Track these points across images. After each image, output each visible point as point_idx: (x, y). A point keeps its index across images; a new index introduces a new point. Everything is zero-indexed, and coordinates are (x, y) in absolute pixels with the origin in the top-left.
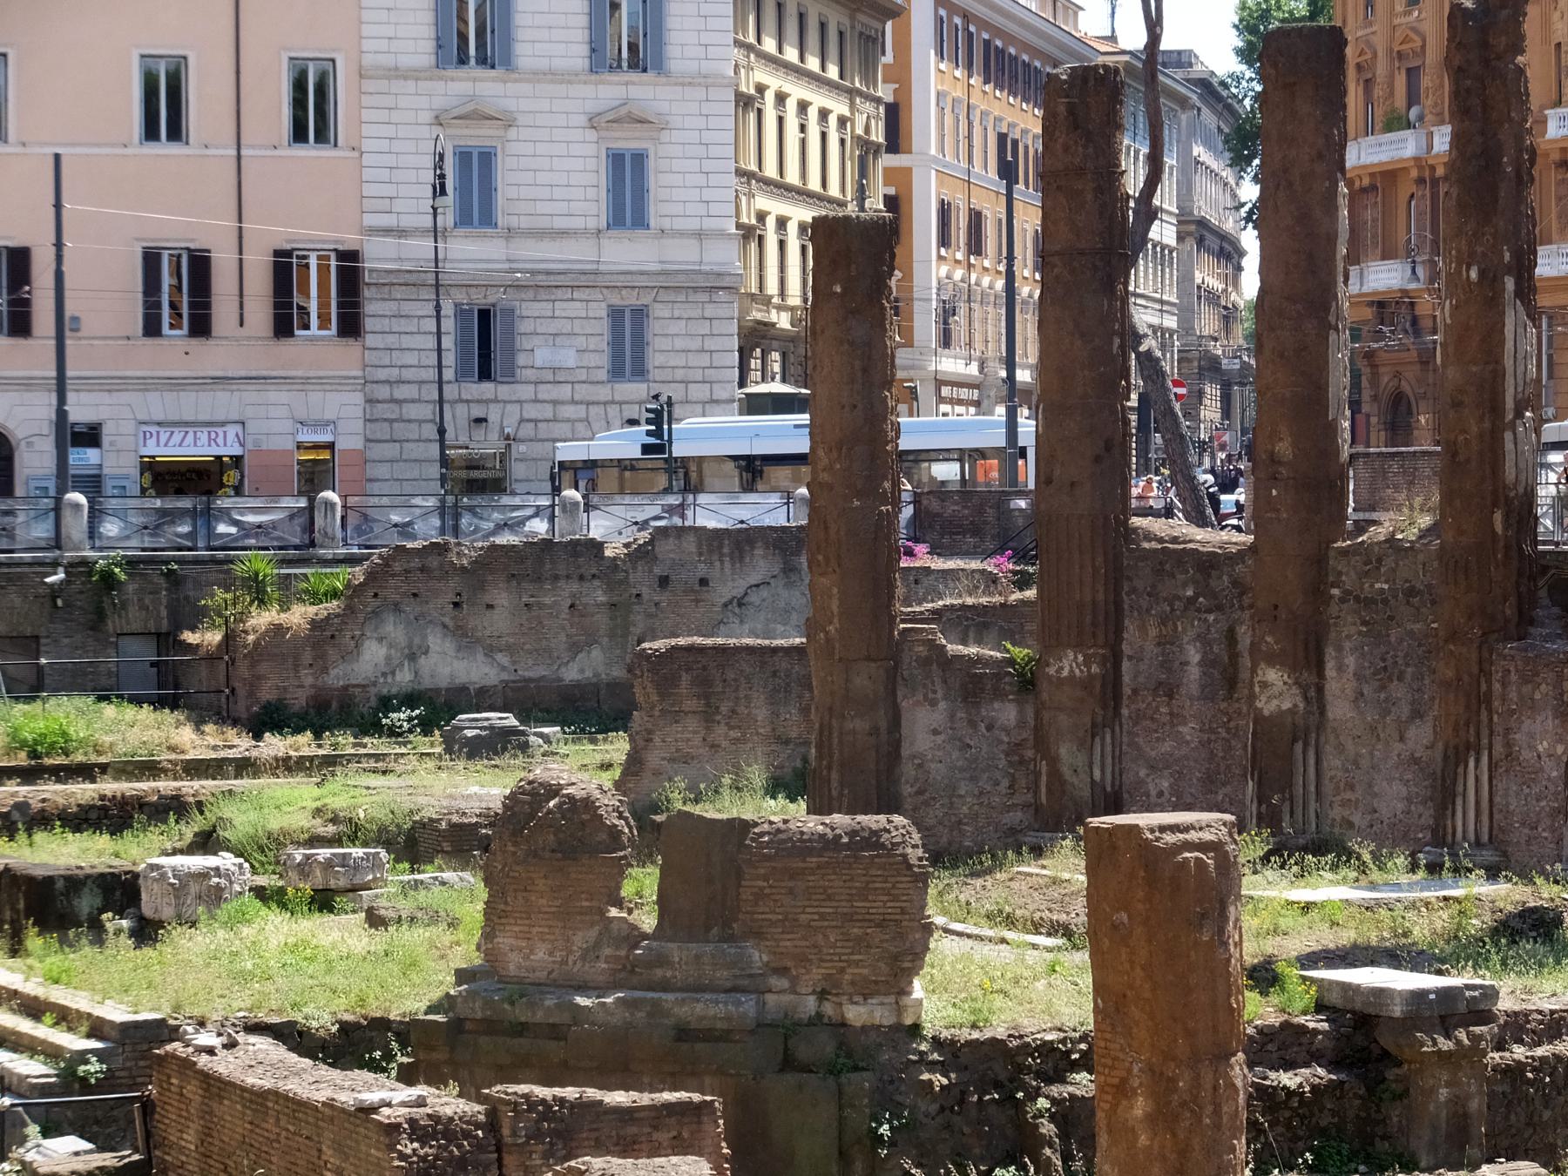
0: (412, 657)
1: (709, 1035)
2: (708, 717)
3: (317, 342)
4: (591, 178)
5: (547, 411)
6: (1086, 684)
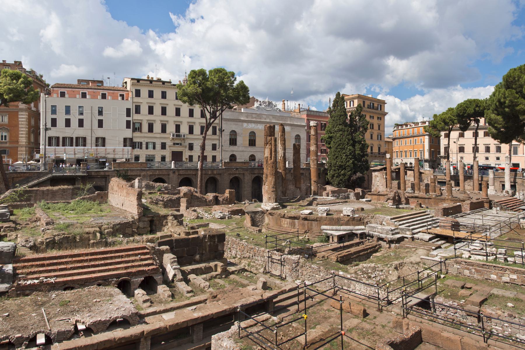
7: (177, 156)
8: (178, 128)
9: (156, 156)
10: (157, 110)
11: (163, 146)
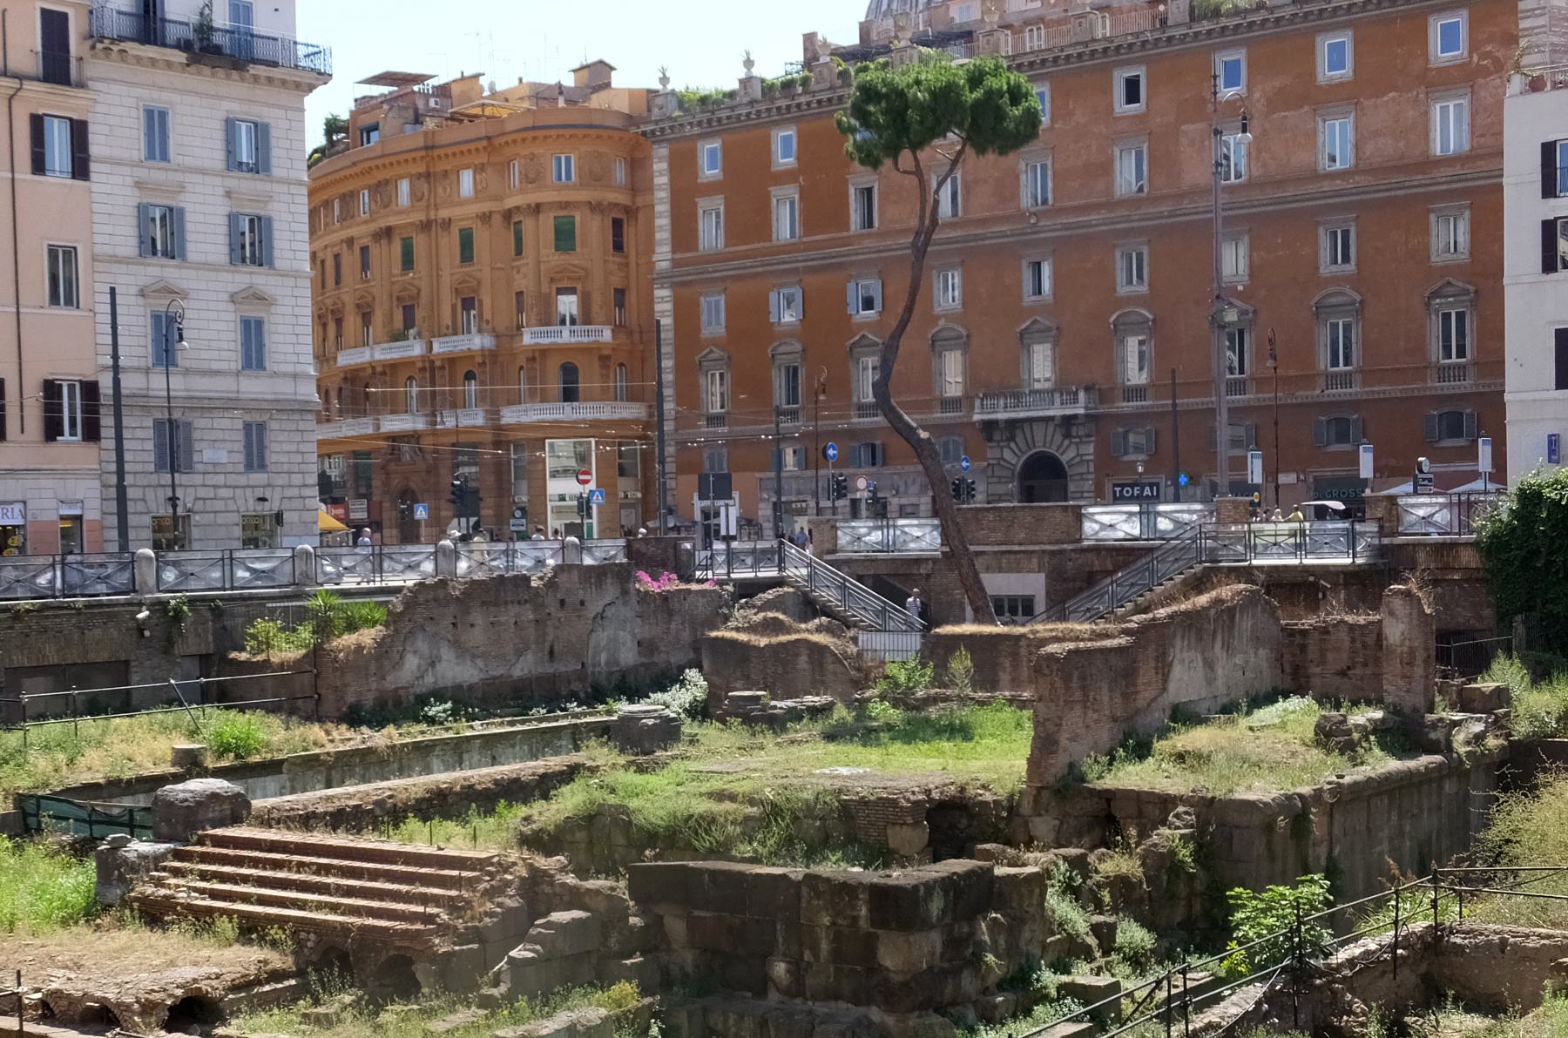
0: (433, 664)
3: (70, 444)
4: (231, 336)
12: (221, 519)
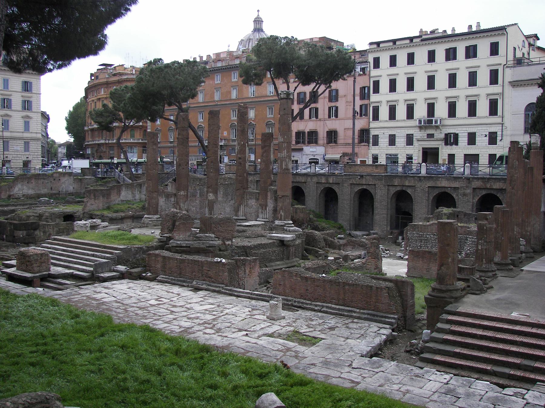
1: (250, 248)
2: (95, 199)
5: (16, 156)
6: (184, 195)
7: (430, 155)
8: (431, 108)
9: (399, 156)
10: (402, 84)
11: (410, 140)
12: (18, 161)
